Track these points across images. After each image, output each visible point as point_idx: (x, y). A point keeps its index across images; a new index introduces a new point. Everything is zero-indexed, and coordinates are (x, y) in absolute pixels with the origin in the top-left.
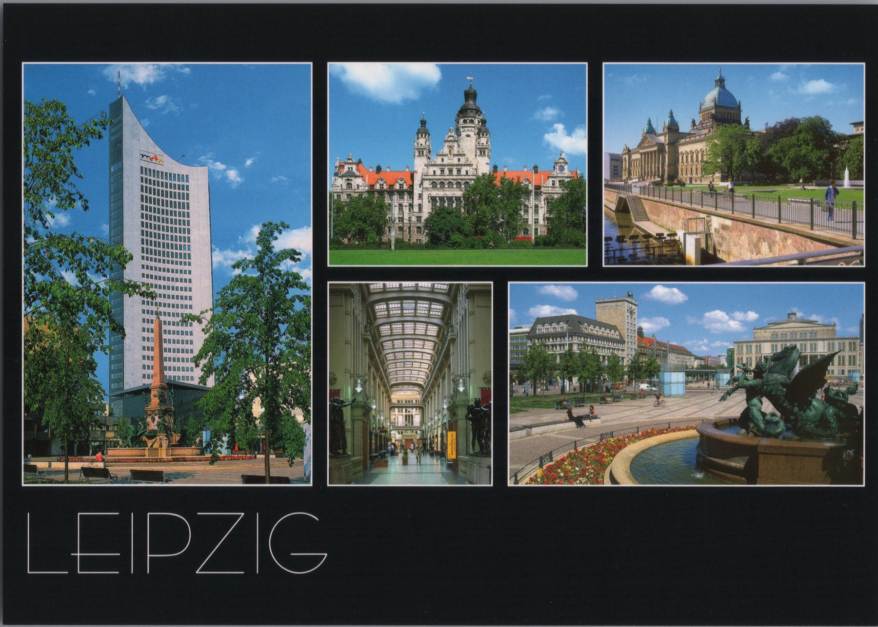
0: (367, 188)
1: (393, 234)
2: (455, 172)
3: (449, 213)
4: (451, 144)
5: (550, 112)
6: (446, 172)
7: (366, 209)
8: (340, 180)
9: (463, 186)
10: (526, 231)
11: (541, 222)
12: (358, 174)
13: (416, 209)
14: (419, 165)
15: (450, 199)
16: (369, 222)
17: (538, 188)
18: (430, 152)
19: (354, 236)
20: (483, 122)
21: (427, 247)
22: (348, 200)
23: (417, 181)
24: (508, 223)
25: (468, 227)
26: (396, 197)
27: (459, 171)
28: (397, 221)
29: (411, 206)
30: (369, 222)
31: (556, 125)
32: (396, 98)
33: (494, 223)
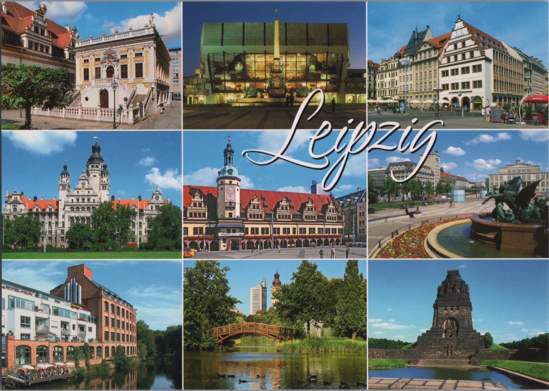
0: (27, 211)
1: (45, 242)
2: (86, 200)
3: (82, 228)
4: (83, 181)
5: (149, 160)
6: (81, 200)
7: (27, 225)
8: (9, 205)
9: (91, 210)
10: (134, 240)
11: (143, 233)
12: (21, 202)
13: (60, 225)
14: (63, 195)
15: (83, 218)
16: (28, 234)
17: (141, 210)
18: (69, 187)
19: (18, 244)
20: (105, 167)
21: (67, 250)
22: (14, 219)
23: (61, 206)
24: (121, 234)
25: (95, 237)
26: (47, 217)
27: (89, 200)
28: (48, 233)
29: (57, 223)
30: (28, 234)
31: (153, 169)
32: (46, 150)
33: (112, 234)
